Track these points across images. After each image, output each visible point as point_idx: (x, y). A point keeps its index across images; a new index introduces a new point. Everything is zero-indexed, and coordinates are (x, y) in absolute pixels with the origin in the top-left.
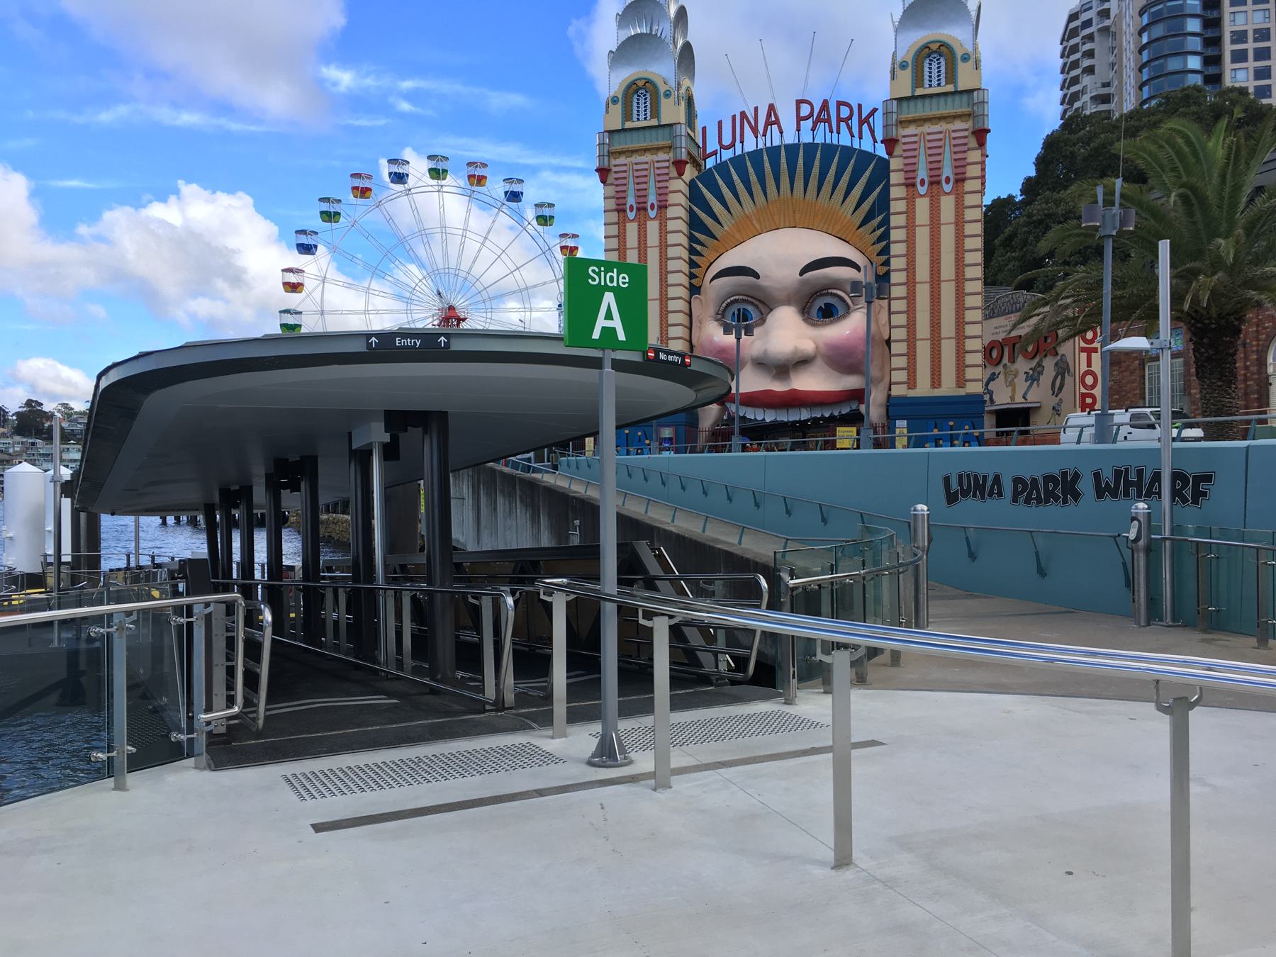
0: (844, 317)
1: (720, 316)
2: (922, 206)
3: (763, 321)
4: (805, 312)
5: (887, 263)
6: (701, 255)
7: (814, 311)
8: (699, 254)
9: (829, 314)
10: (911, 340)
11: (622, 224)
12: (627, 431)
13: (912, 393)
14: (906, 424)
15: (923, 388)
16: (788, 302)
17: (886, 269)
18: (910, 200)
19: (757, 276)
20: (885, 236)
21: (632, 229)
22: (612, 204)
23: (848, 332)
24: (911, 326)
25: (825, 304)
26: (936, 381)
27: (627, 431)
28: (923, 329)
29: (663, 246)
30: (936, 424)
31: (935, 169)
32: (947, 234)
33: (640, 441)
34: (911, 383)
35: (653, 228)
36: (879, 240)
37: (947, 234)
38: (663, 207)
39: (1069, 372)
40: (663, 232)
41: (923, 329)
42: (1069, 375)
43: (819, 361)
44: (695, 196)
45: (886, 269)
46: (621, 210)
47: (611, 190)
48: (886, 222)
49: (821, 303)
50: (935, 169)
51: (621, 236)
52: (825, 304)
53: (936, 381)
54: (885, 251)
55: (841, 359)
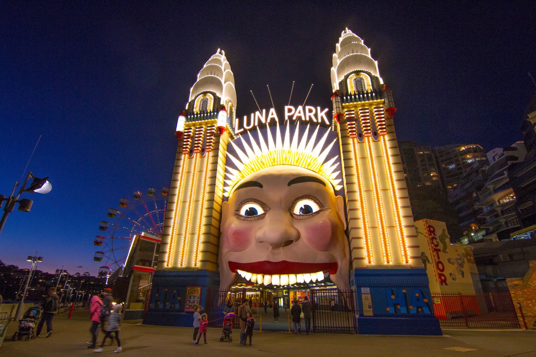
6: (230, 179)
8: (230, 179)
12: (166, 290)
14: (369, 290)
23: (321, 222)
25: (305, 206)
27: (166, 290)
30: (392, 291)
33: (174, 297)
36: (334, 171)
39: (429, 262)
42: (429, 263)
52: (305, 206)
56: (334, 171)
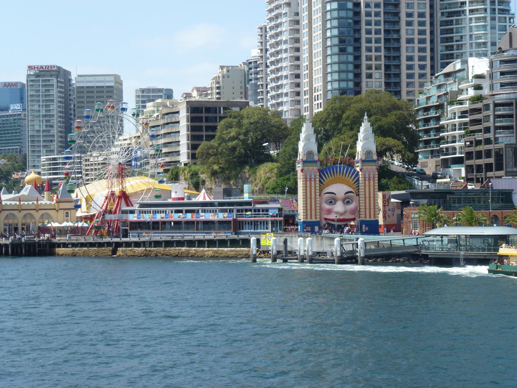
0: (352, 203)
1: (326, 202)
2: (367, 182)
3: (335, 203)
4: (343, 201)
5: (359, 192)
7: (345, 202)
9: (348, 202)
10: (365, 209)
11: (306, 181)
13: (366, 219)
15: (368, 219)
16: (341, 200)
17: (358, 193)
18: (365, 180)
19: (335, 194)
20: (358, 186)
21: (308, 183)
22: (304, 177)
24: (365, 206)
26: (370, 217)
28: (368, 207)
29: (315, 187)
31: (369, 175)
32: (372, 188)
34: (366, 217)
35: (313, 183)
36: (357, 187)
37: (372, 188)
38: (315, 179)
40: (315, 184)
41: (368, 207)
43: (347, 213)
44: (320, 176)
45: (358, 193)
46: (306, 179)
47: (304, 174)
48: (358, 183)
49: (347, 200)
50: (369, 175)
51: (306, 184)
53: (370, 217)
54: (358, 189)
55: (353, 212)
56: (357, 187)
